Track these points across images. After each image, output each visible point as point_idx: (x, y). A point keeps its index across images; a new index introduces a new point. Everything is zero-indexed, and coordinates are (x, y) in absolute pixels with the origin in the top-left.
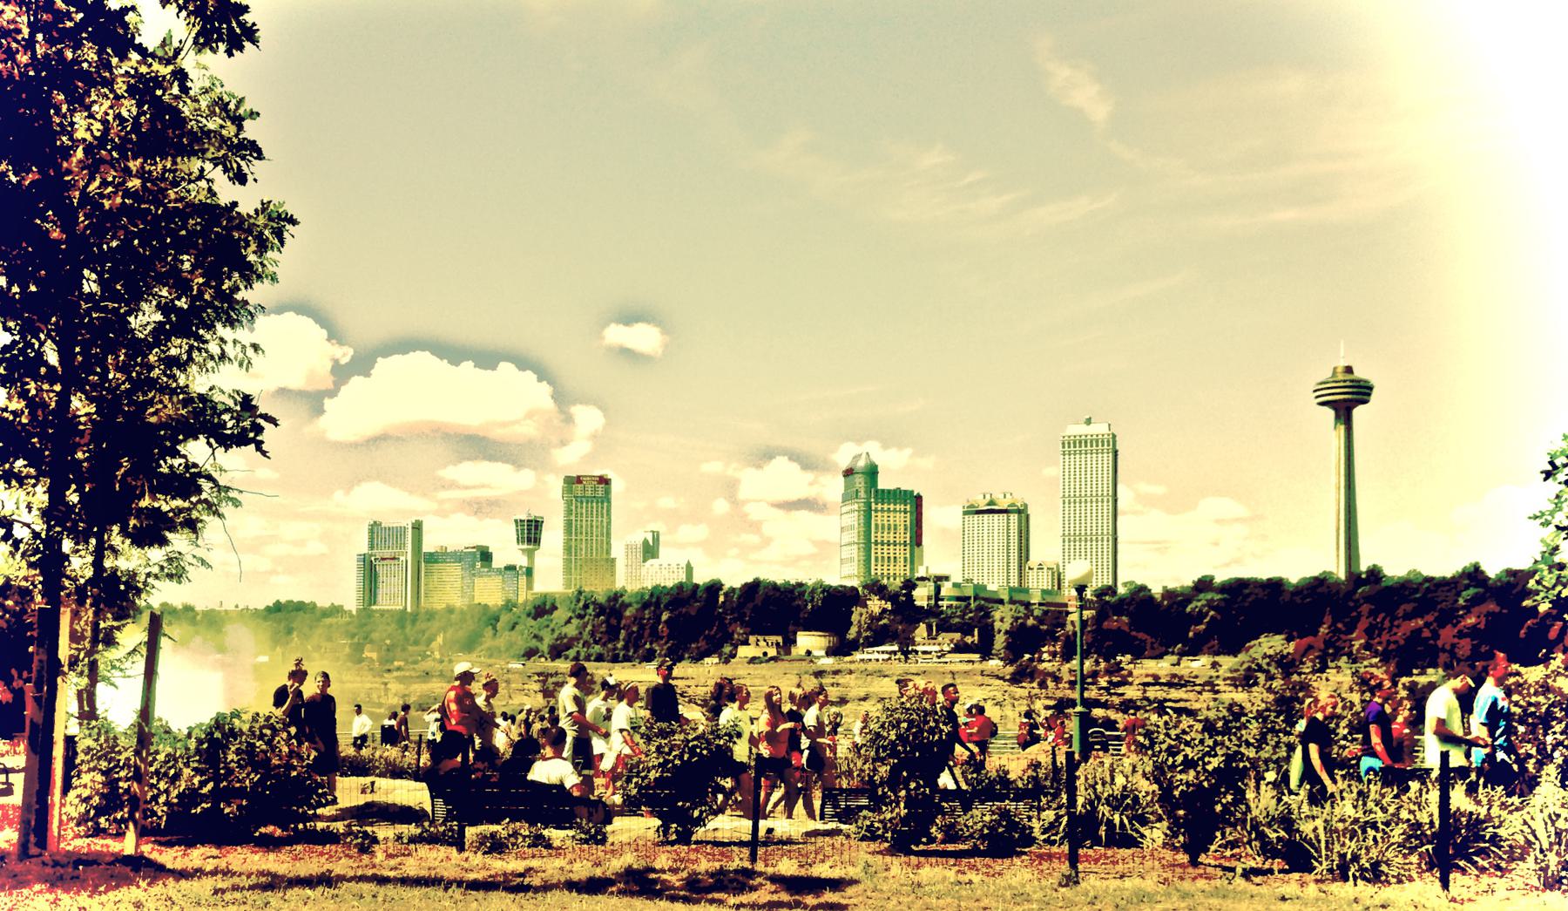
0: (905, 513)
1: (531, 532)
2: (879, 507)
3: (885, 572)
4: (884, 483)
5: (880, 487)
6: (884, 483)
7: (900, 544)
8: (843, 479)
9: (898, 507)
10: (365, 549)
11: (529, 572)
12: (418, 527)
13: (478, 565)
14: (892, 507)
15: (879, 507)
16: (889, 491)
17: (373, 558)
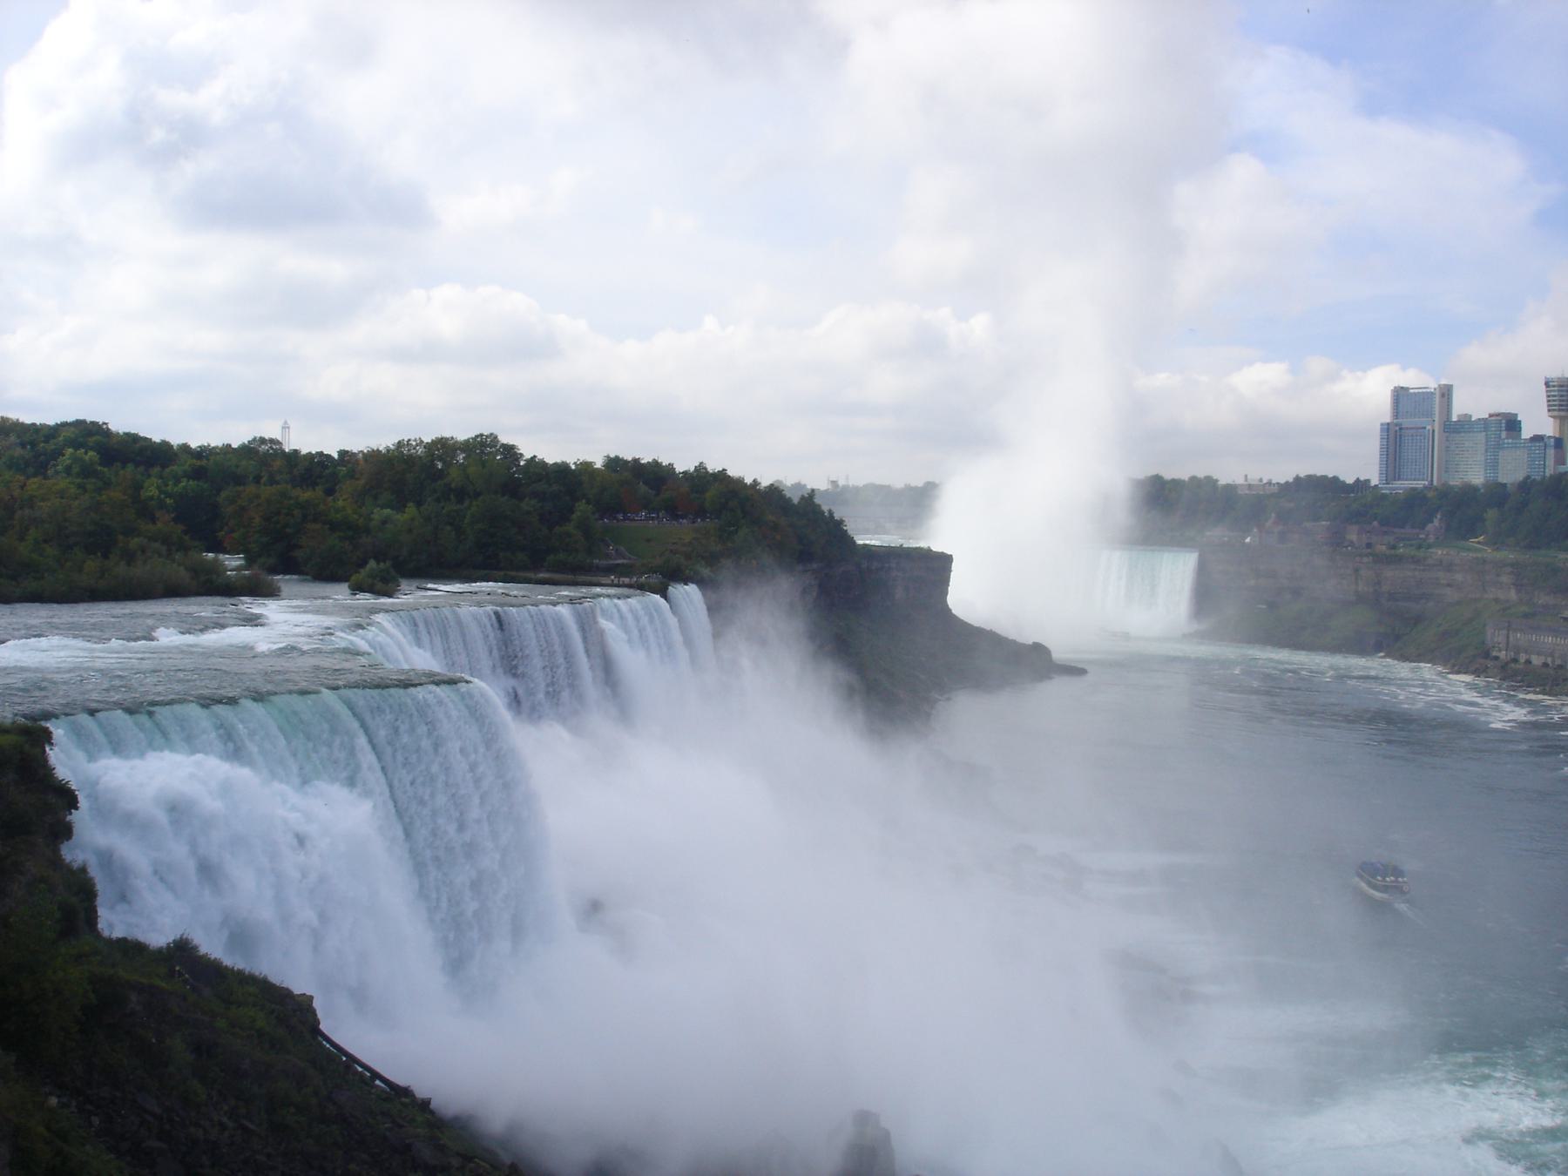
10: (1388, 419)
12: (1446, 393)
13: (1504, 435)
17: (1397, 428)
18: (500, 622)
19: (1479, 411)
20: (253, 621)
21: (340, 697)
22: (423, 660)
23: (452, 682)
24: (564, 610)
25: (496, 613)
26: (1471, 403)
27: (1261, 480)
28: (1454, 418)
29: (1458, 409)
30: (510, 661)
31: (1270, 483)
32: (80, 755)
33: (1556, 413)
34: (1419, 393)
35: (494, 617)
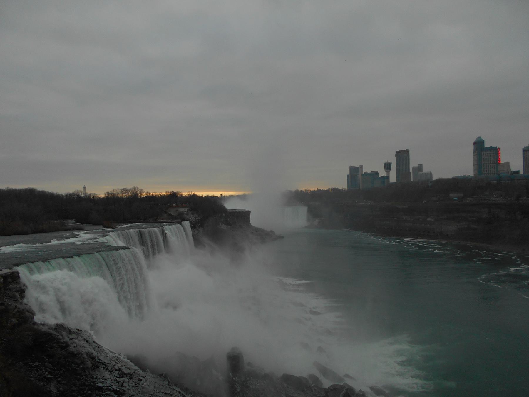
0: (494, 153)
1: (388, 167)
2: (485, 153)
3: (487, 172)
4: (487, 145)
5: (485, 147)
6: (487, 145)
7: (492, 164)
8: (473, 145)
9: (491, 152)
10: (349, 174)
11: (387, 177)
12: (361, 167)
14: (489, 152)
15: (485, 153)
16: (488, 148)
18: (140, 232)
19: (369, 171)
20: (75, 236)
21: (99, 254)
22: (121, 244)
23: (127, 248)
24: (155, 229)
25: (140, 231)
26: (368, 169)
27: (321, 189)
28: (364, 173)
29: (364, 171)
30: (143, 242)
31: (323, 189)
32: (28, 273)
33: (387, 171)
34: (355, 168)
35: (139, 232)
